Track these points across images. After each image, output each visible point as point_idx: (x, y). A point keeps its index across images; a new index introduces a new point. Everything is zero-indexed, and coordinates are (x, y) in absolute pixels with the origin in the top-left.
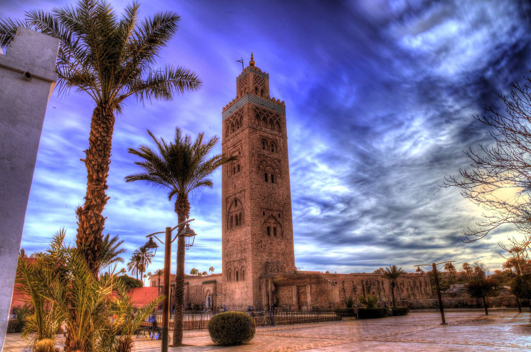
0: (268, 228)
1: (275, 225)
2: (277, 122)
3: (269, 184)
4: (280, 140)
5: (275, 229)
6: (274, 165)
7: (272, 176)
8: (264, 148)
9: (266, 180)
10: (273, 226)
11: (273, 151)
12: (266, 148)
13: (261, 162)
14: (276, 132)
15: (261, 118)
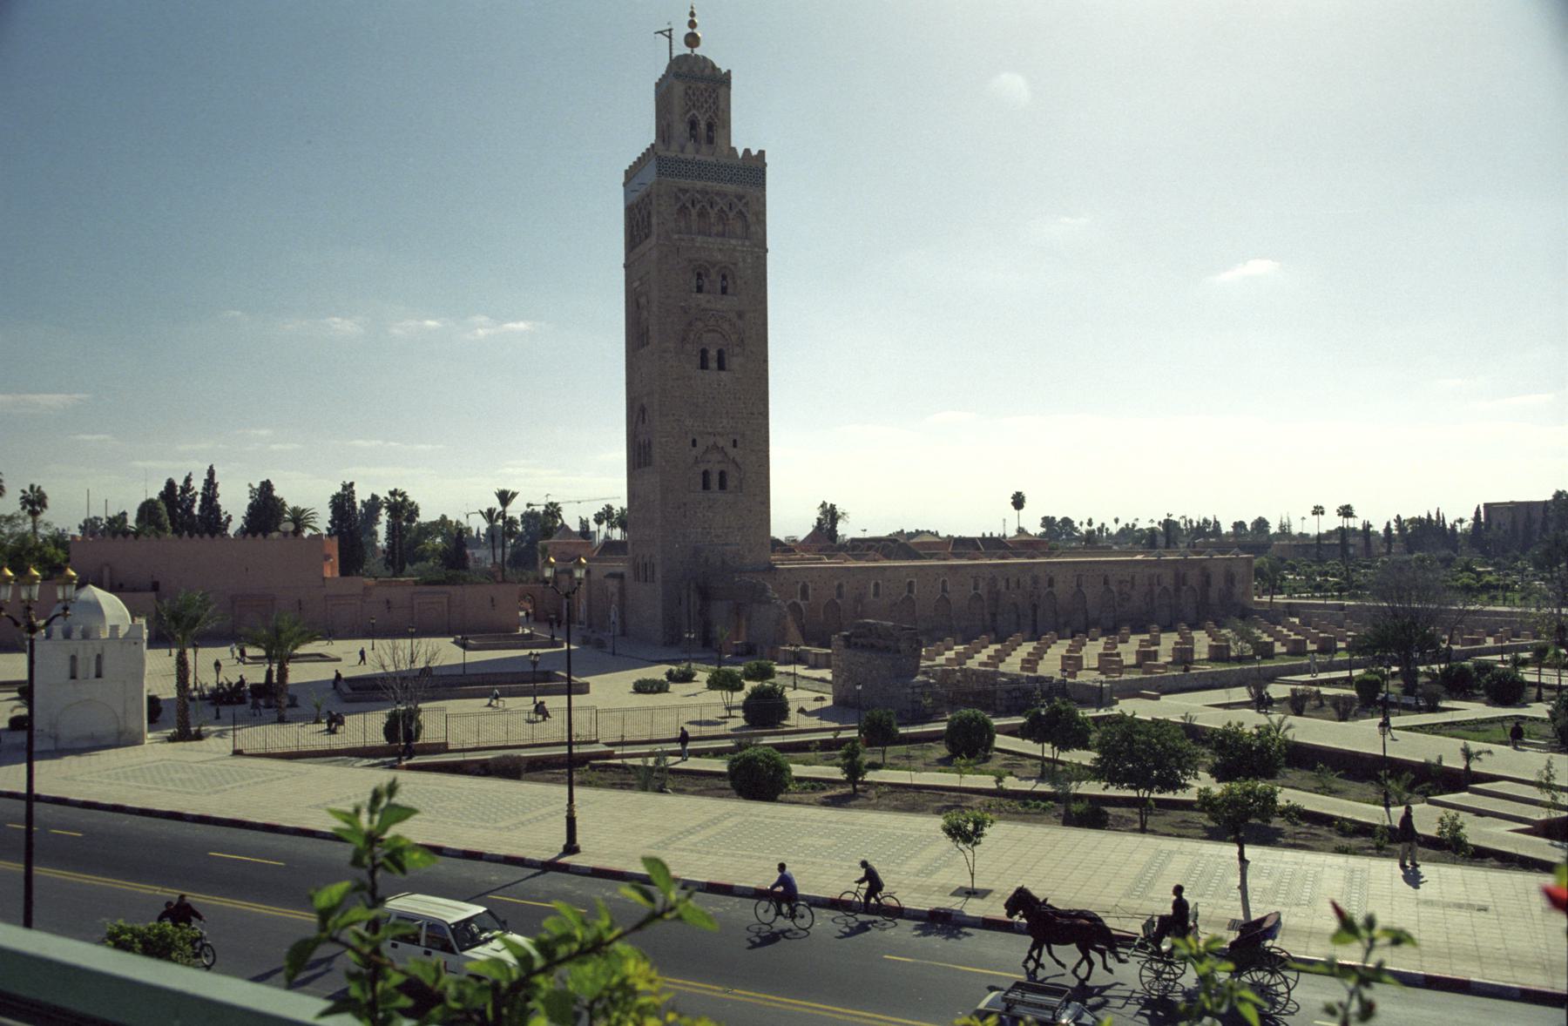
0: (706, 474)
1: (722, 467)
2: (741, 212)
3: (712, 375)
4: (744, 261)
5: (722, 474)
6: (726, 326)
7: (720, 353)
8: (700, 289)
9: (704, 365)
10: (715, 469)
11: (724, 291)
12: (706, 286)
13: (690, 324)
14: (733, 242)
15: (694, 212)
